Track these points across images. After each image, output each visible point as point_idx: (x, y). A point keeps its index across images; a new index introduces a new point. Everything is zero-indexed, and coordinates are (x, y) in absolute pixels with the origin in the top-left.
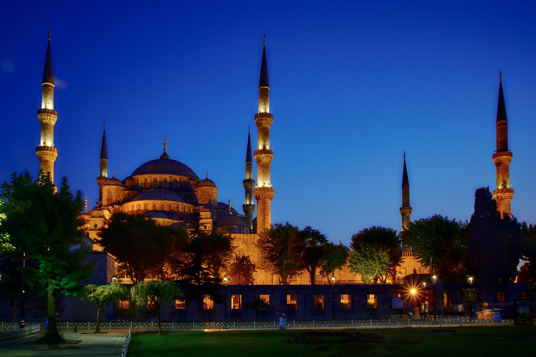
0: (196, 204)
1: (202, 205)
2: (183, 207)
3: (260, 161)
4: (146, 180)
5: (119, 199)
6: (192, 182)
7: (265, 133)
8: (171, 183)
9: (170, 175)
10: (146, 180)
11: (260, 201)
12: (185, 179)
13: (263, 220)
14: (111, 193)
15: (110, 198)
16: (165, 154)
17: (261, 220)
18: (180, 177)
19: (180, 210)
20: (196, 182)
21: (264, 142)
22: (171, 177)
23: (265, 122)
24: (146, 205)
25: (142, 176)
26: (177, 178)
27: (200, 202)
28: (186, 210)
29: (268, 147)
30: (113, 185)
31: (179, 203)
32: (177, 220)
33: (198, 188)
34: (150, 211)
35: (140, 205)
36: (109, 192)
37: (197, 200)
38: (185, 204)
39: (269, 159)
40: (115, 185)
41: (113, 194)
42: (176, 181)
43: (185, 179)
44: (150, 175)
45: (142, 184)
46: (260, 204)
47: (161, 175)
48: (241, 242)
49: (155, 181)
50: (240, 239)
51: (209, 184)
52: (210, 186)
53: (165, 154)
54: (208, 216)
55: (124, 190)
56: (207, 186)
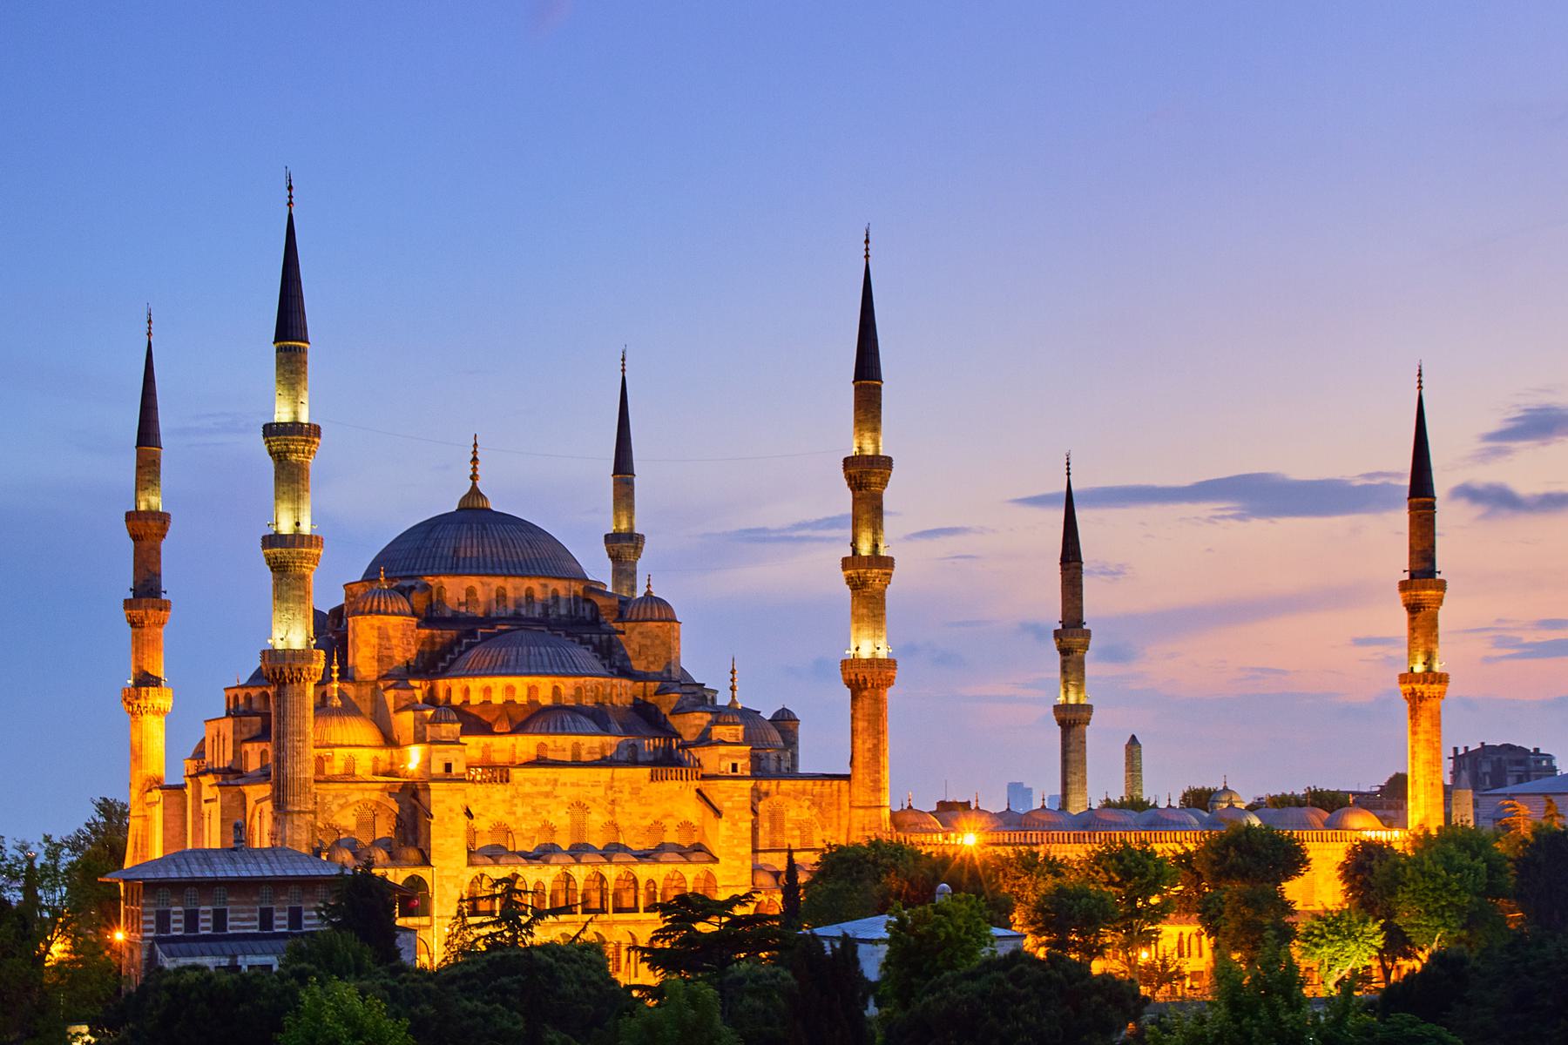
3: (864, 584)
4: (470, 592)
5: (408, 656)
9: (543, 581)
11: (865, 693)
13: (876, 746)
14: (388, 639)
15: (385, 652)
16: (475, 492)
17: (869, 745)
18: (566, 583)
22: (545, 586)
24: (532, 690)
25: (456, 580)
30: (394, 614)
33: (628, 625)
36: (383, 635)
37: (626, 658)
40: (400, 614)
41: (394, 642)
44: (486, 579)
45: (460, 604)
46: (867, 702)
47: (518, 581)
48: (807, 803)
50: (804, 793)
53: (475, 492)
55: (418, 626)
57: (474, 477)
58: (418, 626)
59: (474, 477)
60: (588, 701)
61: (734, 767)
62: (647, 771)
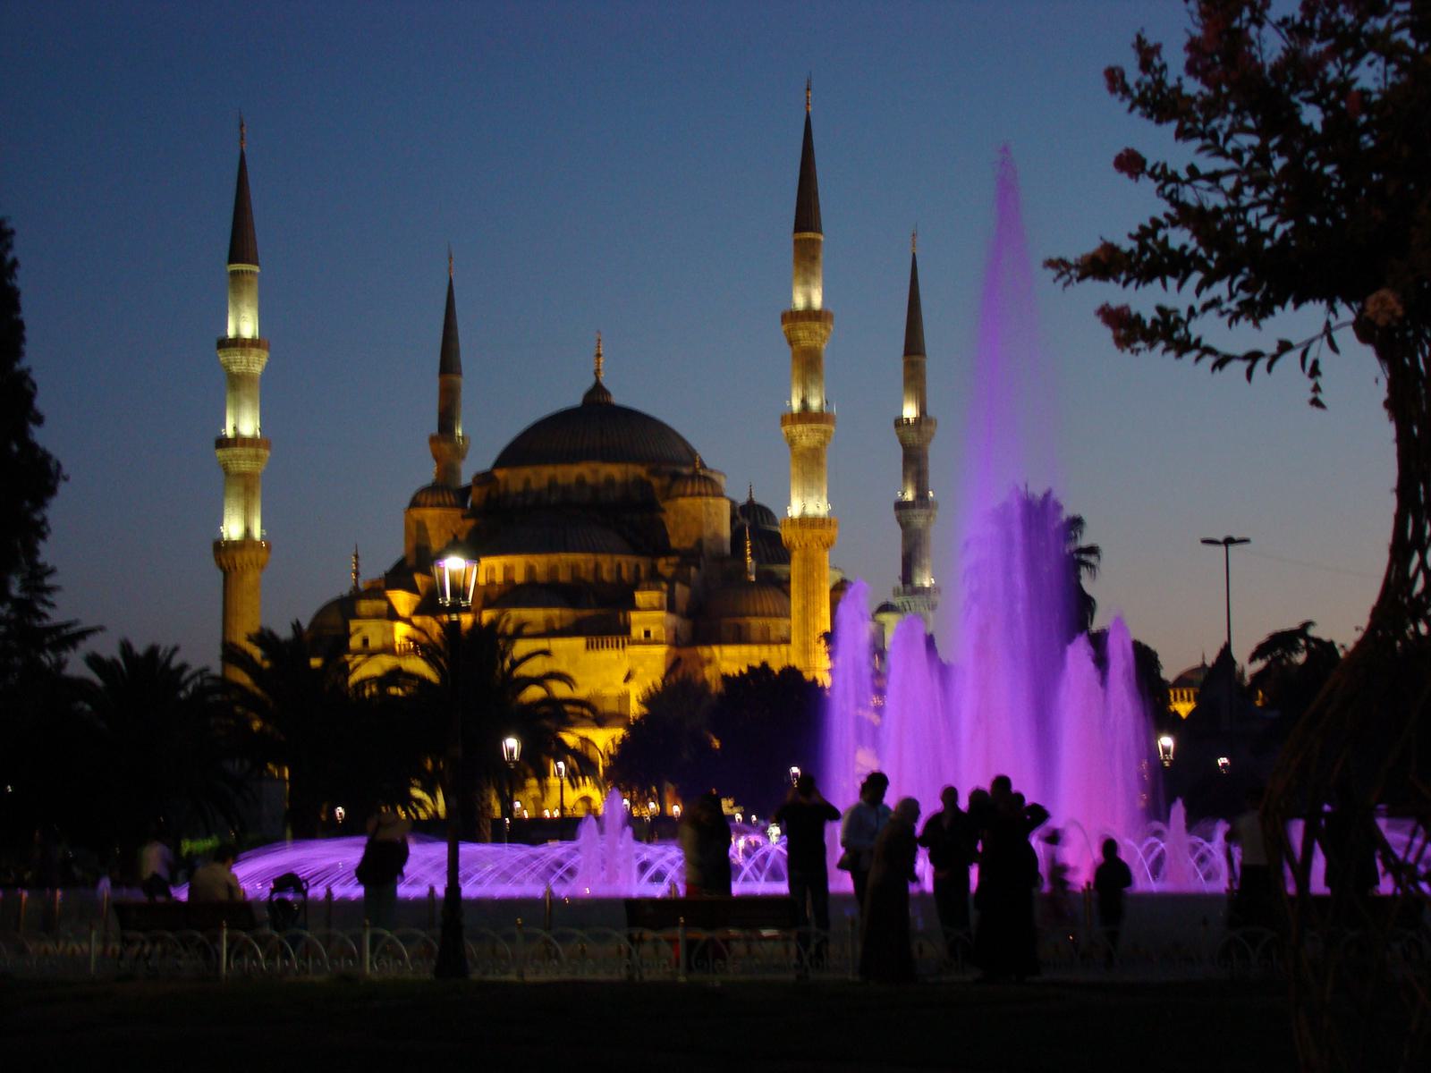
0: (664, 549)
1: (674, 552)
2: (610, 564)
4: (527, 482)
6: (656, 482)
7: (809, 364)
8: (595, 489)
10: (527, 482)
12: (641, 471)
19: (606, 576)
20: (666, 481)
21: (805, 388)
23: (806, 334)
26: (616, 471)
27: (674, 543)
28: (625, 574)
29: (815, 403)
31: (600, 558)
32: (589, 607)
34: (521, 586)
35: (493, 570)
37: (666, 536)
38: (618, 558)
39: (818, 437)
40: (439, 505)
41: (431, 533)
42: (610, 481)
43: (641, 471)
49: (552, 484)
51: (696, 489)
52: (700, 494)
54: (656, 604)
55: (463, 517)
56: (692, 495)
57: (597, 372)
58: (463, 517)
59: (597, 372)
60: (564, 576)
61: (647, 633)
62: (580, 642)
